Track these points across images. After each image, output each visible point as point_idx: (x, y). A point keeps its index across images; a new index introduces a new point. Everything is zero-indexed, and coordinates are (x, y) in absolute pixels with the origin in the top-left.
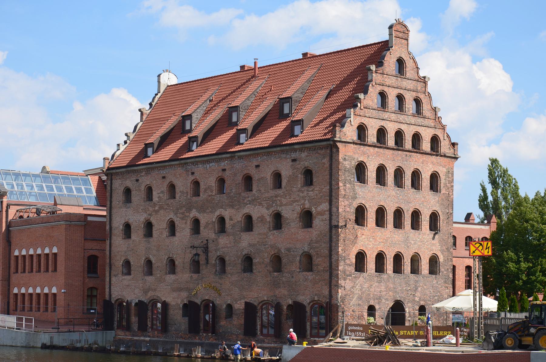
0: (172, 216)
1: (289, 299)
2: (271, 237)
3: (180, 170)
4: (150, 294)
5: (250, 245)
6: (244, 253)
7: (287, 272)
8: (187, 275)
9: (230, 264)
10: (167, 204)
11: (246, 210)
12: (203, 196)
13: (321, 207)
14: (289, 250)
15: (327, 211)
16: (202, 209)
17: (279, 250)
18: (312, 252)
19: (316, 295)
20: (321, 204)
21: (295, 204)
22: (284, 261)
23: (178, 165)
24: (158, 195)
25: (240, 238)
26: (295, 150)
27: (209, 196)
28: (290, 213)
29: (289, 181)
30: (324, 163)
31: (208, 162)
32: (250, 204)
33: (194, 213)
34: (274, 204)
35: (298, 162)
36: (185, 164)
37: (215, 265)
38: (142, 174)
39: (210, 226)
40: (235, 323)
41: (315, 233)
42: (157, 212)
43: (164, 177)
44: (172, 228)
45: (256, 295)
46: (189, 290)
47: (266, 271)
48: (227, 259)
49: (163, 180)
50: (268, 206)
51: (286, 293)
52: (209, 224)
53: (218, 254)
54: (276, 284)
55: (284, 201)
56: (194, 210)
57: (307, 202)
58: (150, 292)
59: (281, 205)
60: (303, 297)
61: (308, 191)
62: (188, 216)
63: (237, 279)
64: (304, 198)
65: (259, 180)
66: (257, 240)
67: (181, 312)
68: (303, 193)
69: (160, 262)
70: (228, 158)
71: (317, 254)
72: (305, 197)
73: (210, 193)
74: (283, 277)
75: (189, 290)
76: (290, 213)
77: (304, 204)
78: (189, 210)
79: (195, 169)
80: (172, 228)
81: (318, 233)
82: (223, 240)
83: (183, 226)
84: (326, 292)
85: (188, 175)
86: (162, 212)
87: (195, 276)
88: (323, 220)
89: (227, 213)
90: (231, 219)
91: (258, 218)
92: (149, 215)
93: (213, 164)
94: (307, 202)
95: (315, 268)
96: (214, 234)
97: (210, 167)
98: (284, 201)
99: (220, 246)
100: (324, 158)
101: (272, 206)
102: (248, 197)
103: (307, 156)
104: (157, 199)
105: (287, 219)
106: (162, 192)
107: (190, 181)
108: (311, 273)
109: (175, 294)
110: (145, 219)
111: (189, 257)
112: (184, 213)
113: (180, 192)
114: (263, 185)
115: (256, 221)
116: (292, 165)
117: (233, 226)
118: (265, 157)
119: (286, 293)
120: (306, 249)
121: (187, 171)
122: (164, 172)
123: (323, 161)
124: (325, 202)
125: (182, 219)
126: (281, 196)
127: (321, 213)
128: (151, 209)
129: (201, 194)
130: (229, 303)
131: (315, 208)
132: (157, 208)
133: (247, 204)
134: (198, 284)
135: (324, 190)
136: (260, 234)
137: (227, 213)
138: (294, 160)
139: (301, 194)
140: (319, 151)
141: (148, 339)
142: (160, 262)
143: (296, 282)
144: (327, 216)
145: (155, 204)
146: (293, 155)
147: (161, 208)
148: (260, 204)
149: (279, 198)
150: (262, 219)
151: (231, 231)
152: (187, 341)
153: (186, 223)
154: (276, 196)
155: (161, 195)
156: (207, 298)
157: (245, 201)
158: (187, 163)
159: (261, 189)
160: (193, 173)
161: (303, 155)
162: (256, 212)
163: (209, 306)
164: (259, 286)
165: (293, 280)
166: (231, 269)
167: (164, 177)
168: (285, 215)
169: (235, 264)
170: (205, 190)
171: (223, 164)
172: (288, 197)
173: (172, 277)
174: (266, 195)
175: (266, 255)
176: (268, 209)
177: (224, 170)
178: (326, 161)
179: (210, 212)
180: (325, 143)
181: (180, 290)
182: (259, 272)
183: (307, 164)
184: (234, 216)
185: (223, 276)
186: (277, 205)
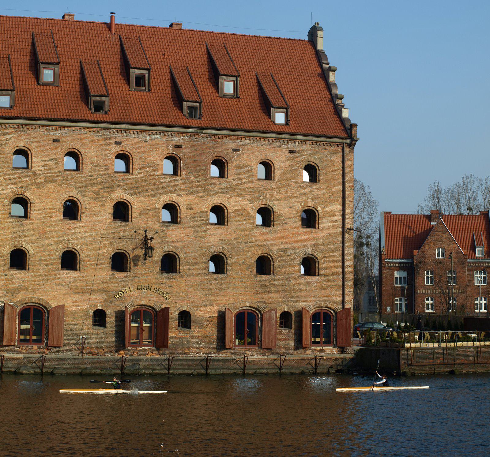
0: (73, 193)
1: (285, 305)
2: (257, 234)
3: (89, 135)
4: (20, 296)
5: (222, 241)
6: (212, 250)
7: (281, 276)
8: (105, 273)
9: (187, 262)
10: (63, 177)
11: (216, 200)
12: (137, 174)
13: (330, 207)
14: (284, 251)
15: (338, 212)
16: (137, 189)
17: (269, 250)
18: (318, 255)
19: (323, 301)
20: (330, 204)
21: (293, 200)
22: (277, 263)
23: (92, 128)
24: (43, 163)
25: (206, 232)
26: (295, 140)
27: (150, 175)
28: (288, 210)
29: (284, 174)
30: (334, 162)
31: (149, 132)
32: (222, 192)
33: (119, 195)
34: (262, 197)
35: (298, 155)
36: (104, 128)
37: (156, 262)
38: (7, 131)
39: (151, 213)
40: (195, 333)
41: (322, 235)
42: (39, 185)
43: (57, 141)
44: (71, 210)
45: (232, 300)
46: (105, 291)
47: (249, 273)
48: (182, 255)
49: (56, 144)
50: (252, 198)
51: (280, 298)
52: (149, 210)
53: (166, 248)
54: (263, 289)
55: (277, 195)
56: (119, 190)
57: (310, 200)
58: (22, 293)
59: (272, 199)
60: (305, 303)
61: (312, 188)
62: (107, 197)
63: (198, 281)
64: (306, 195)
65: (238, 166)
66: (234, 236)
67: (91, 320)
68: (305, 189)
69: (44, 251)
70: (187, 133)
71: (325, 257)
72: (308, 194)
73: (151, 172)
74: (276, 280)
75: (105, 291)
76: (288, 210)
77: (306, 202)
78: (111, 189)
79: (119, 137)
80: (71, 210)
81: (325, 234)
82: (174, 233)
83: (97, 208)
84: (338, 298)
85: (109, 145)
86: (51, 186)
87: (120, 275)
88: (332, 222)
89: (183, 199)
90: (189, 207)
91: (236, 210)
92: (22, 187)
93: (158, 136)
94: (310, 200)
95: (321, 272)
96: (158, 224)
97: (151, 139)
98: (277, 195)
99: (169, 240)
100: (334, 156)
101: (259, 199)
102: (220, 184)
103: (311, 150)
104: (43, 169)
105: (282, 216)
106: (53, 160)
107: (113, 152)
108: (316, 277)
109: (78, 297)
110: (13, 192)
111: (108, 251)
112: (99, 191)
113: (93, 164)
114: (244, 174)
115: (232, 214)
116: (290, 157)
117: (194, 217)
118: (248, 141)
119: (280, 298)
120: (310, 251)
121: (106, 138)
122: (58, 134)
123: (333, 159)
124: (335, 203)
125: (95, 199)
126: (273, 189)
127: (331, 214)
128: (26, 180)
129: (135, 172)
130: (185, 309)
131: (322, 208)
132: (40, 180)
133: (218, 193)
134: (126, 285)
135: (334, 190)
136: (239, 229)
137: (182, 201)
138: (292, 152)
139: (302, 191)
140: (327, 148)
141: (21, 356)
142: (44, 251)
143: (294, 286)
144: (340, 219)
145: (36, 175)
146: (291, 146)
147: (48, 180)
148: (239, 195)
149: (269, 191)
150: (242, 212)
151: (191, 222)
152: (104, 357)
153: (103, 205)
154: (265, 188)
155: (51, 164)
156: (143, 303)
157: (215, 189)
158: (108, 128)
159: (242, 177)
160: (118, 143)
161: (306, 148)
162: (231, 204)
163: (142, 313)
164: (237, 290)
165: (291, 284)
166: (188, 269)
167: (57, 141)
168: (278, 211)
169: (197, 263)
170: (143, 168)
171: (176, 139)
172: (282, 191)
173: (71, 273)
174: (250, 185)
175: (249, 255)
176: (252, 201)
177: (180, 147)
178: (337, 159)
179: (151, 195)
180: (340, 140)
181: (91, 292)
182: (238, 273)
183: (310, 158)
184: (194, 204)
185: (174, 277)
186: (265, 197)
